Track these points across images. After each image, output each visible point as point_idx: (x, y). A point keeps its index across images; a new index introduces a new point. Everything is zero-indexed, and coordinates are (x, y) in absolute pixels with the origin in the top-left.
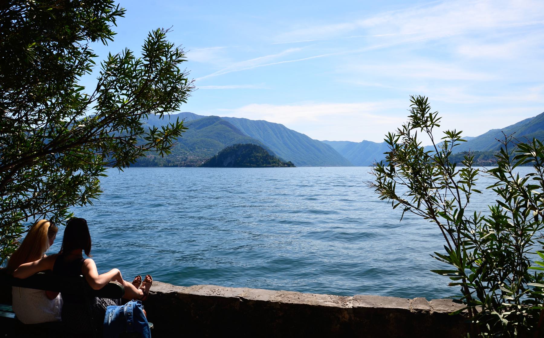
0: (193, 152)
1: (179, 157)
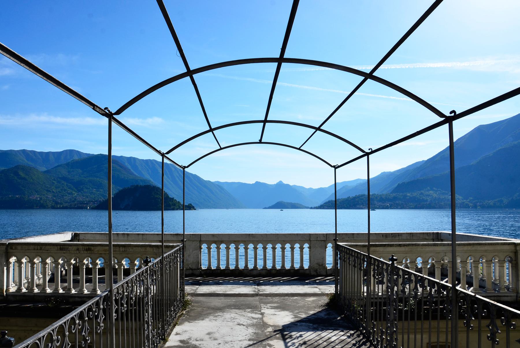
1: (67, 198)
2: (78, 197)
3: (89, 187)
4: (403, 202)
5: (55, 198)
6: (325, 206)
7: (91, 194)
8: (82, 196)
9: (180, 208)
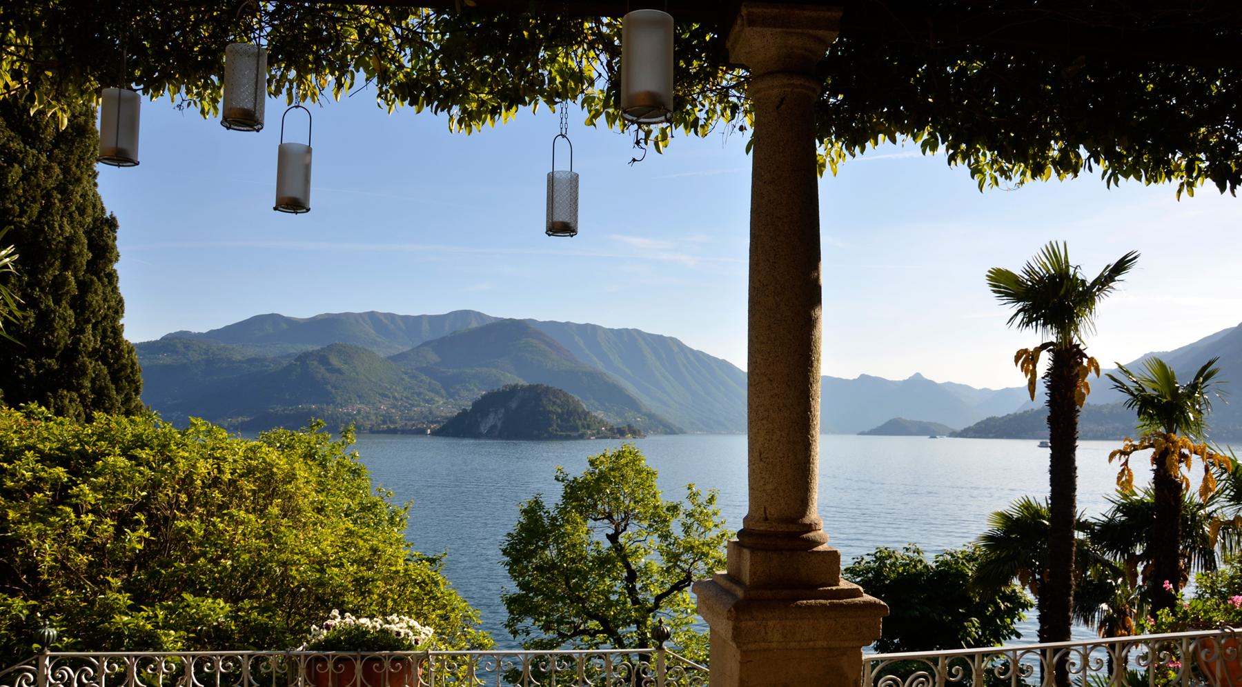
0: (455, 400)
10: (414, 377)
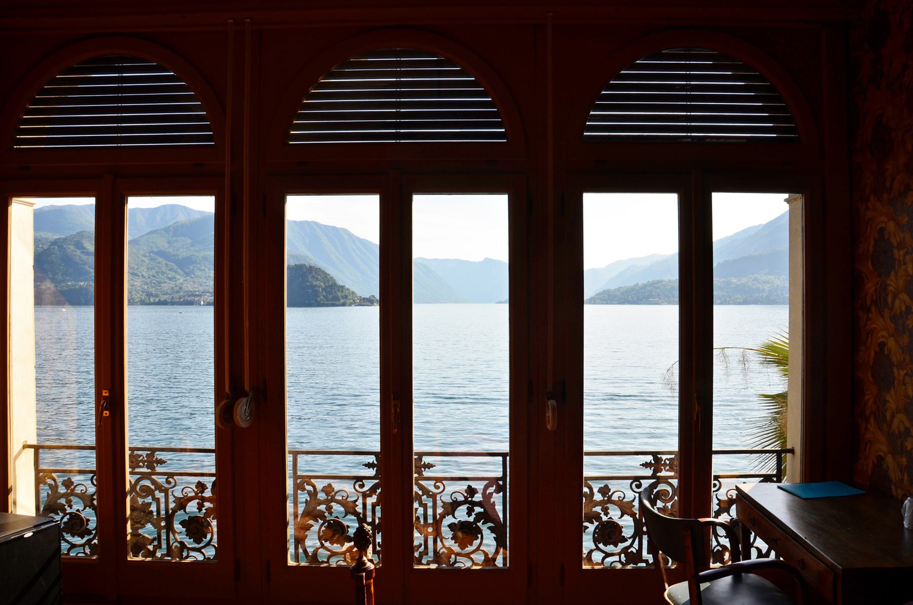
0: (191, 278)
1: (166, 286)
2: (185, 285)
3: (203, 268)
4: (725, 293)
5: (146, 287)
6: (598, 299)
7: (207, 280)
8: (192, 283)
9: (355, 303)
10: (152, 259)
